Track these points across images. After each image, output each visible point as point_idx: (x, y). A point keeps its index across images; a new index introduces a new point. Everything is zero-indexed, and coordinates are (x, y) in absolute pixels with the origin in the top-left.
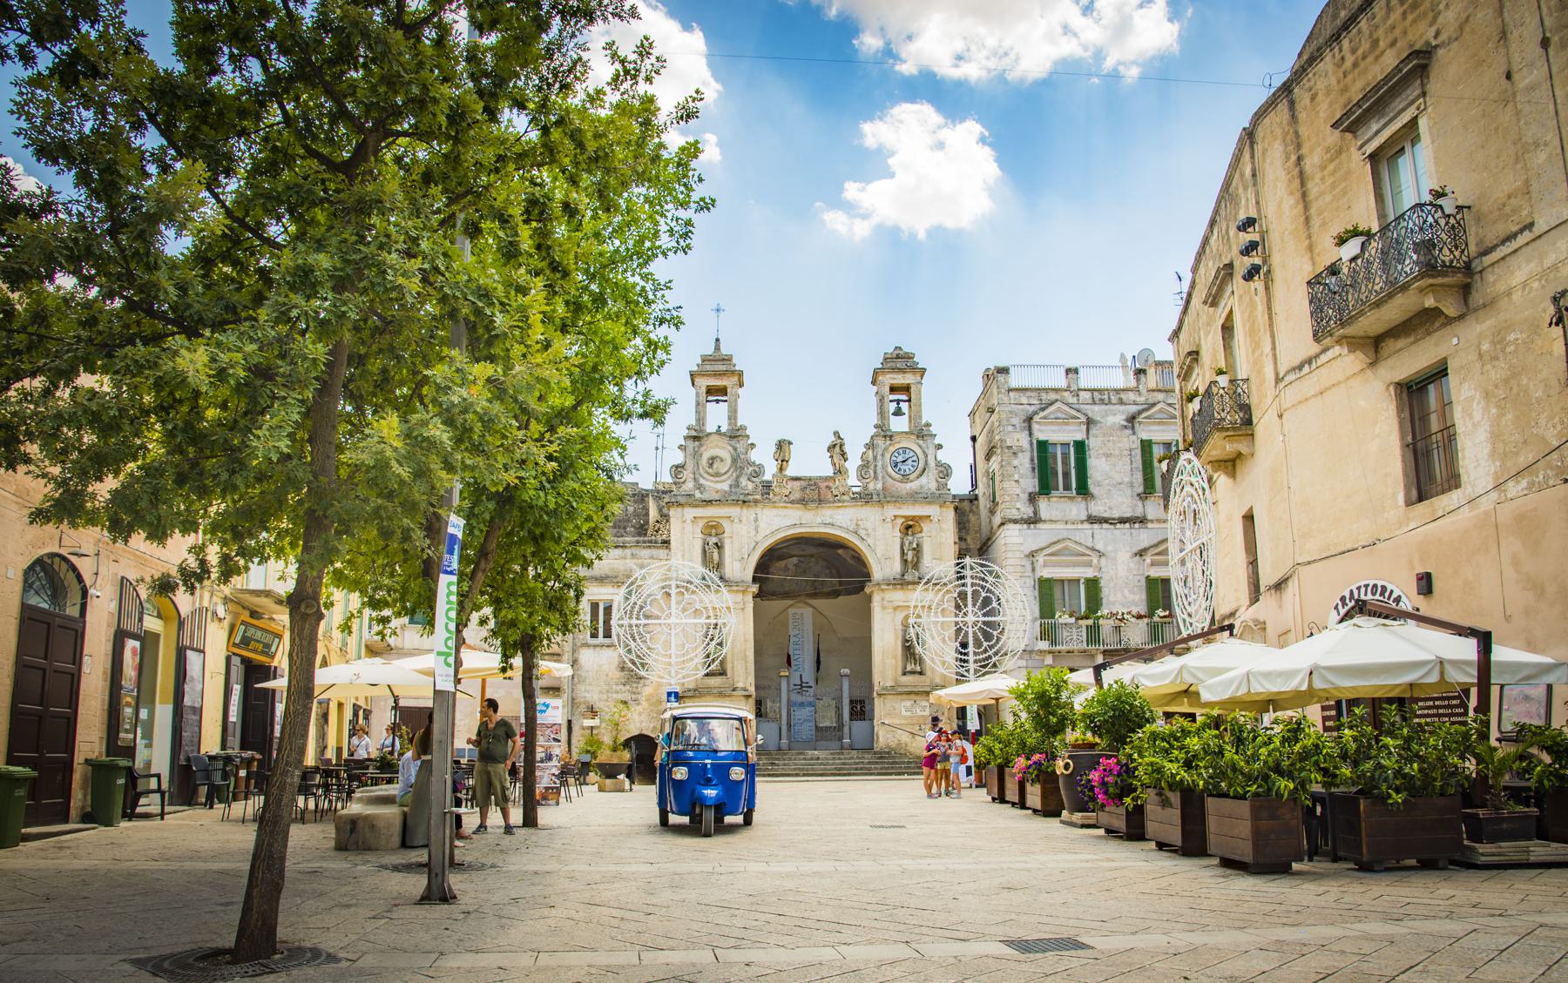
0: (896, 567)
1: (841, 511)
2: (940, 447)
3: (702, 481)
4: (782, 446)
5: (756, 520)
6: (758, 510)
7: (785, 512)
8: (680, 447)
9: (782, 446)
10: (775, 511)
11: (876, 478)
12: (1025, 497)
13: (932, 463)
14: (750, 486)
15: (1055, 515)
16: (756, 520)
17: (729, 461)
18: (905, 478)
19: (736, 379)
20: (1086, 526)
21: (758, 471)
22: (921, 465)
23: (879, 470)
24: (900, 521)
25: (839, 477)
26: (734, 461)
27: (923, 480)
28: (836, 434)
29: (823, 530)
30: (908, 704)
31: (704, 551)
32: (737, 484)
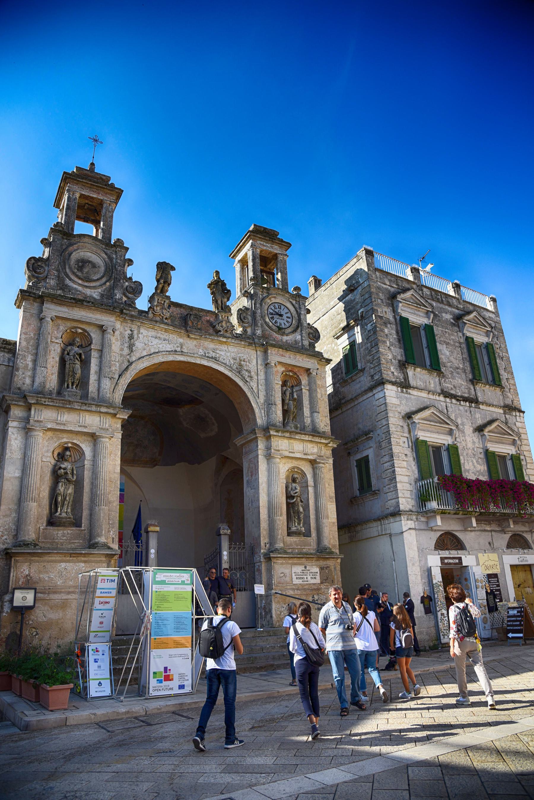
0: (278, 414)
1: (224, 347)
3: (68, 282)
5: (131, 337)
6: (134, 327)
7: (165, 335)
8: (44, 242)
10: (152, 333)
12: (395, 362)
15: (420, 384)
16: (131, 337)
17: (103, 269)
20: (442, 398)
23: (258, 318)
24: (281, 369)
25: (222, 316)
28: (217, 273)
29: (205, 363)
30: (298, 569)
31: (63, 362)
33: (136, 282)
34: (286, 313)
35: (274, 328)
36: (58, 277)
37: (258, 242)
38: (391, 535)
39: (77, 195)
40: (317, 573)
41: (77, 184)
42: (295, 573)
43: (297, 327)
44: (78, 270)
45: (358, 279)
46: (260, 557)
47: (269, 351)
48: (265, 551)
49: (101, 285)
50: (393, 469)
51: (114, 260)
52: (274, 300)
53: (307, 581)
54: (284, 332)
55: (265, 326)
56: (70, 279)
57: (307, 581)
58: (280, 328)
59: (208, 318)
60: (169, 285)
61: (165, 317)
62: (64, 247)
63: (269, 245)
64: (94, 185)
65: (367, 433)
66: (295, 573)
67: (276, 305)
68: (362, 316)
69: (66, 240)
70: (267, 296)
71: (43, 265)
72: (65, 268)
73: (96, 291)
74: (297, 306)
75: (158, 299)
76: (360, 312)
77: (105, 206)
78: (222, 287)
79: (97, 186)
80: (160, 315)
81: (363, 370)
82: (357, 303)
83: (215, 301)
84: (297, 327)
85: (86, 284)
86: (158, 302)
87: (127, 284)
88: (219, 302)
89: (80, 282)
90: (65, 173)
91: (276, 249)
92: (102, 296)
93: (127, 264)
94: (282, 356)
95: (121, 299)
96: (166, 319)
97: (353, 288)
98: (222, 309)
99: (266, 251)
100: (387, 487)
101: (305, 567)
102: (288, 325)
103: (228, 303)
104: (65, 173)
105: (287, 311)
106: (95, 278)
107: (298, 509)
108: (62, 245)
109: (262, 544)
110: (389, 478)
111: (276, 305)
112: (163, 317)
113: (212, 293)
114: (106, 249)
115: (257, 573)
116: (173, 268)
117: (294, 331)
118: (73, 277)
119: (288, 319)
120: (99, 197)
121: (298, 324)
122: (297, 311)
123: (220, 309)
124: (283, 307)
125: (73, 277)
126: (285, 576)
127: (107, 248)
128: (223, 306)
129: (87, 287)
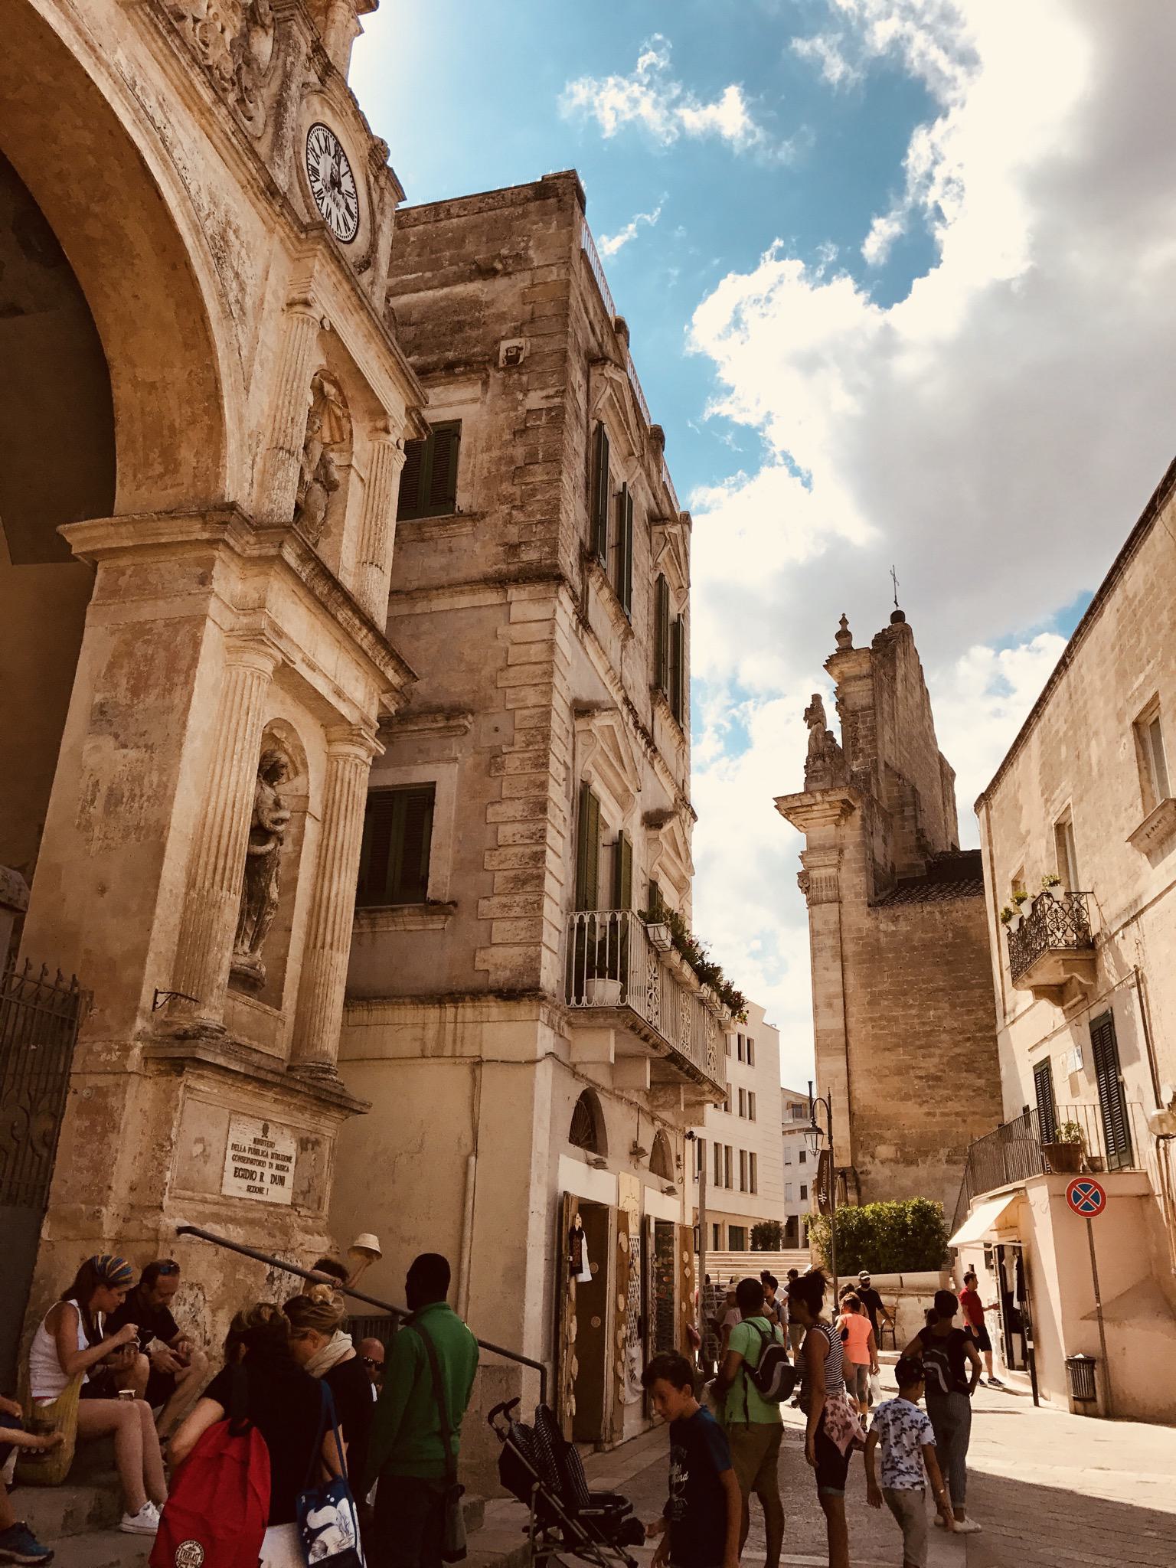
38: (478, 1063)
40: (289, 1159)
42: (234, 1146)
45: (526, 248)
46: (126, 1049)
48: (149, 1028)
50: (538, 848)
53: (261, 1190)
57: (261, 1190)
65: (454, 712)
66: (234, 1146)
68: (512, 360)
76: (504, 345)
81: (474, 517)
82: (501, 317)
97: (499, 266)
100: (495, 900)
101: (265, 1130)
107: (268, 886)
109: (146, 999)
110: (512, 873)
115: (72, 1124)
126: (205, 1156)
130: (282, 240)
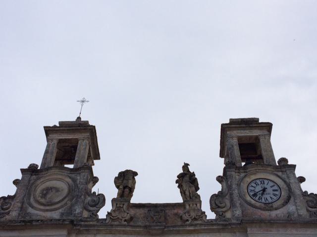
2: (302, 179)
3: (30, 210)
4: (126, 181)
8: (16, 182)
9: (126, 181)
11: (233, 205)
13: (298, 192)
14: (86, 214)
17: (66, 191)
18: (268, 207)
19: (88, 134)
21: (100, 200)
22: (284, 194)
26: (71, 190)
27: (291, 208)
28: (186, 166)
32: (70, 211)
33: (99, 195)
34: (271, 187)
35: (258, 204)
36: (22, 208)
37: (235, 132)
39: (55, 142)
41: (56, 133)
43: (289, 198)
44: (41, 197)
47: (249, 229)
49: (62, 207)
51: (78, 181)
52: (253, 177)
54: (272, 207)
55: (246, 205)
56: (33, 207)
58: (265, 204)
59: (176, 211)
60: (131, 190)
61: (124, 219)
62: (32, 182)
63: (247, 131)
64: (70, 130)
67: (258, 182)
69: (34, 176)
70: (245, 176)
71: (10, 201)
72: (30, 199)
73: (56, 211)
74: (284, 176)
75: (117, 204)
77: (79, 142)
78: (190, 179)
79: (72, 130)
80: (118, 218)
83: (183, 193)
84: (289, 198)
85: (48, 208)
86: (117, 207)
87: (89, 198)
88: (187, 193)
89: (42, 207)
90: (45, 127)
91: (255, 133)
92: (62, 214)
93: (91, 183)
94: (267, 231)
95: (81, 213)
96: (125, 221)
98: (191, 198)
99: (246, 137)
102: (275, 198)
103: (198, 192)
104: (45, 127)
105: (272, 184)
106: (57, 200)
108: (29, 181)
111: (258, 182)
112: (121, 220)
113: (179, 187)
114: (71, 173)
116: (135, 174)
117: (287, 202)
118: (35, 205)
119: (276, 193)
120: (75, 137)
121: (289, 194)
122: (285, 182)
123: (188, 199)
124: (266, 182)
125: (35, 205)
127: (72, 172)
128: (191, 195)
129: (47, 210)
130: (239, 232)
